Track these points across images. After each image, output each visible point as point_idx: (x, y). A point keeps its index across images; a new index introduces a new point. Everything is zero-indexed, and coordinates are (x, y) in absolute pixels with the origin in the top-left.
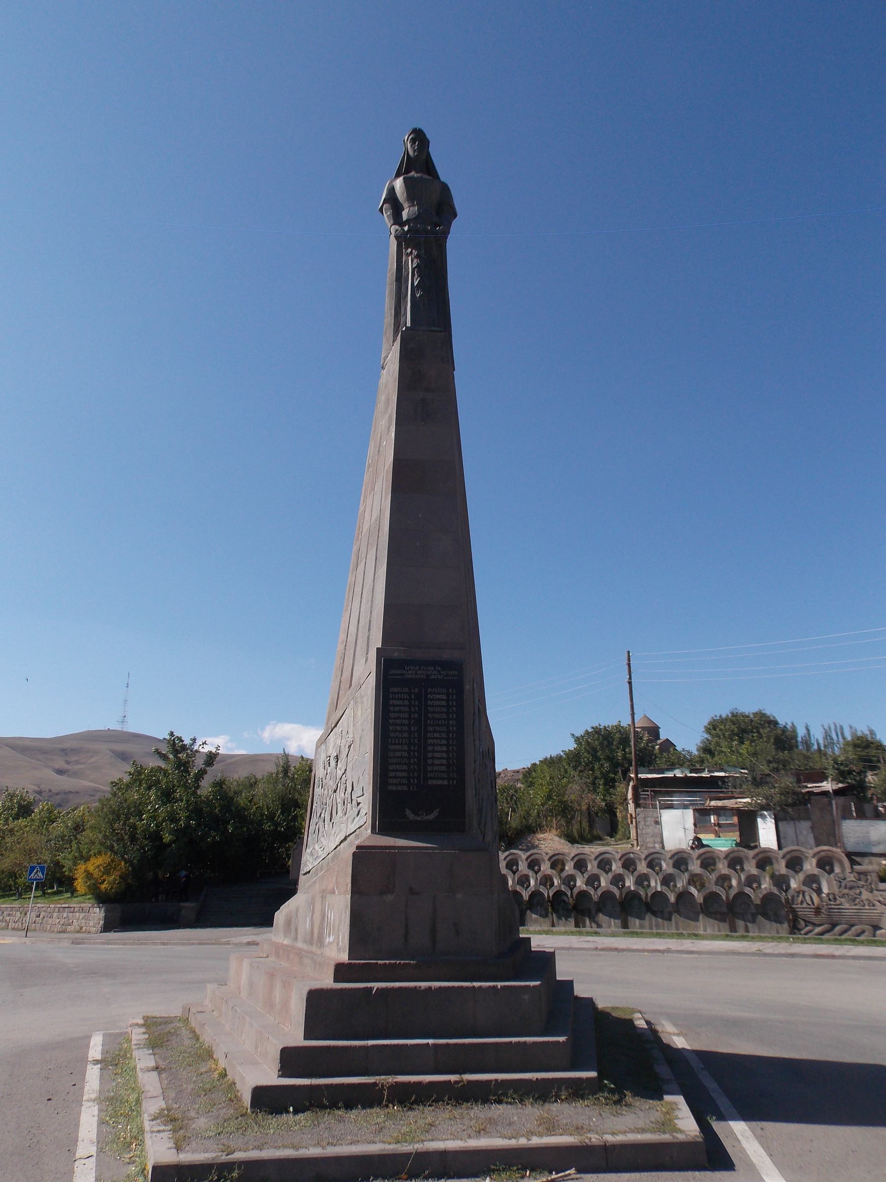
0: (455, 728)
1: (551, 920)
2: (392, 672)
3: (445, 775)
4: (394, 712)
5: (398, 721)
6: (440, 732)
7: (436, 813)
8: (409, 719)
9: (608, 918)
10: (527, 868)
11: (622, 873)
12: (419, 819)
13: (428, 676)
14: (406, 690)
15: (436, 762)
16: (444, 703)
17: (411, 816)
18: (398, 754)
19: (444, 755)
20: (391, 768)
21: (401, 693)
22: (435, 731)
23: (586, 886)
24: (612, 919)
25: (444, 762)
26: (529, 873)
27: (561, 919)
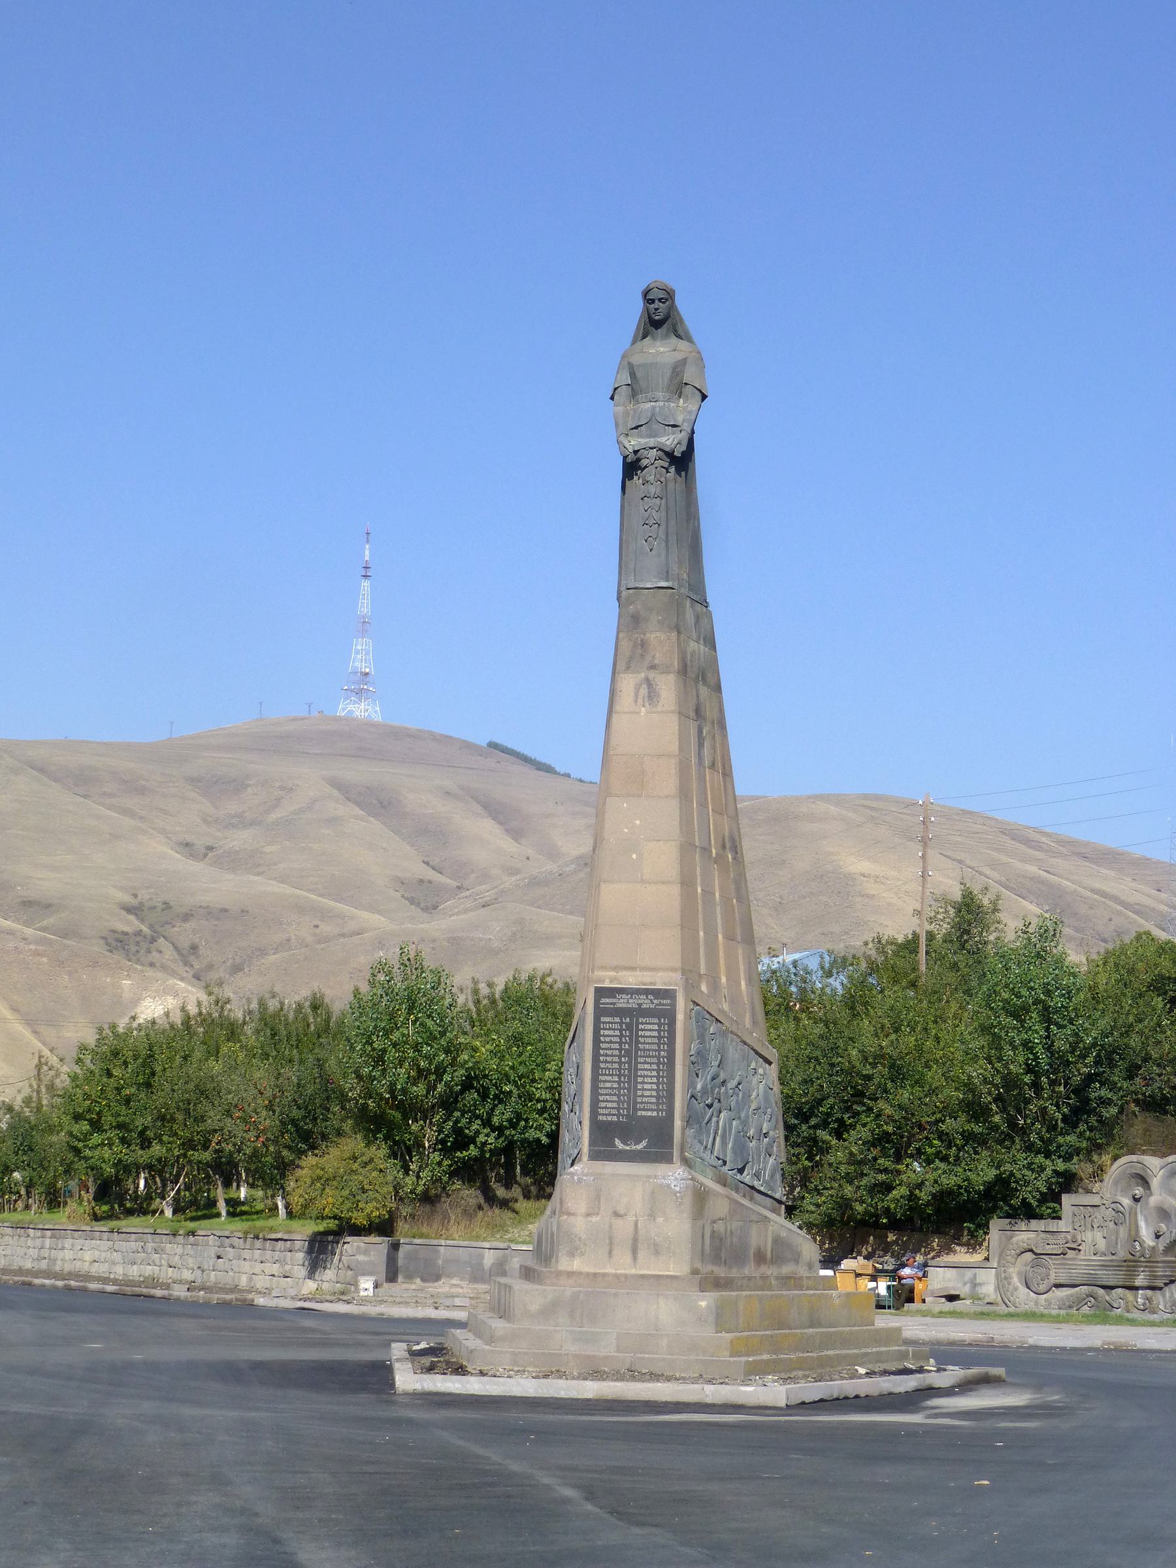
0: (665, 1060)
2: (603, 1000)
3: (654, 1107)
4: (605, 1042)
5: (609, 1052)
6: (651, 1063)
7: (644, 1143)
8: (620, 1050)
12: (628, 1148)
13: (639, 1004)
14: (617, 1019)
15: (647, 1093)
16: (655, 1034)
17: (619, 1144)
18: (608, 1085)
19: (655, 1087)
20: (601, 1098)
21: (612, 1023)
22: (645, 1063)
25: (654, 1093)
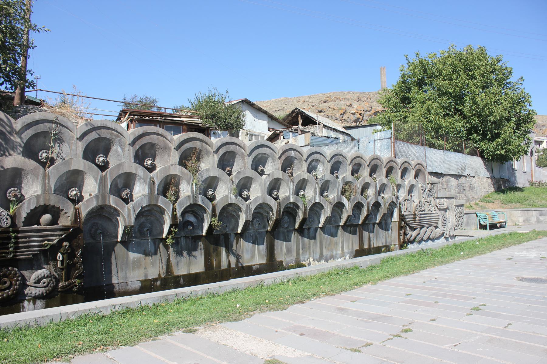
1: (164, 261)
9: (251, 245)
10: (132, 160)
11: (281, 178)
23: (236, 197)
24: (256, 246)
26: (136, 170)
27: (182, 255)
